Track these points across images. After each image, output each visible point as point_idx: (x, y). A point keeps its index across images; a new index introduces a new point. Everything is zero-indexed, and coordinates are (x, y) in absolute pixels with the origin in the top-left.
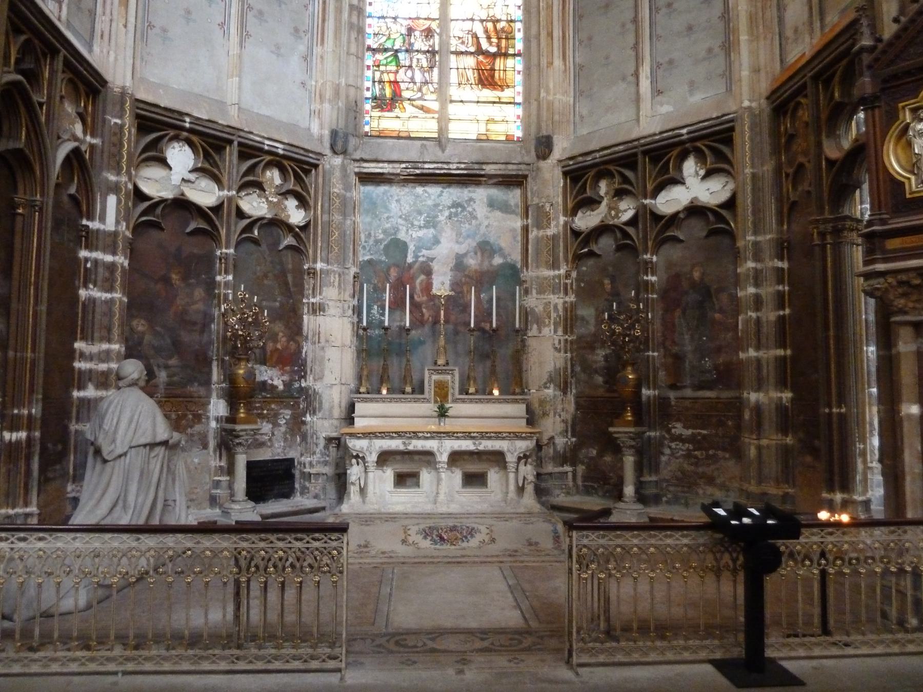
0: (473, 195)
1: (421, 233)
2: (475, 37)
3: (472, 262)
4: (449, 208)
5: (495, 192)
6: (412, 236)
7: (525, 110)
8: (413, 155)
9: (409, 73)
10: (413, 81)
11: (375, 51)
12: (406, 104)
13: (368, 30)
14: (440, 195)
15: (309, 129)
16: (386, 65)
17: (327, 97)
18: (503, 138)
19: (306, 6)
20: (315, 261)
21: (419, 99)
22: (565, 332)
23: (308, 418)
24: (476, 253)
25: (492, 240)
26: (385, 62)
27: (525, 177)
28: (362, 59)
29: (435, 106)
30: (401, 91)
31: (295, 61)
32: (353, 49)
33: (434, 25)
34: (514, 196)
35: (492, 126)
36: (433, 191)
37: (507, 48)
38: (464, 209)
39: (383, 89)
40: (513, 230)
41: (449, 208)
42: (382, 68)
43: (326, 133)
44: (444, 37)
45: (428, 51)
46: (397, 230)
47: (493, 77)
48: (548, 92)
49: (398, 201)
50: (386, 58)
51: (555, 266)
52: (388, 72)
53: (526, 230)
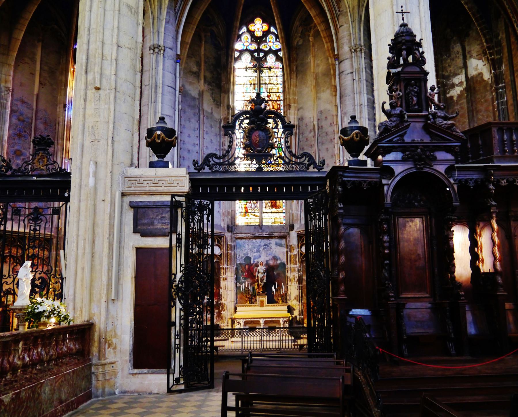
3: (271, 263)
5: (277, 240)
6: (252, 255)
7: (286, 215)
8: (252, 231)
9: (250, 205)
12: (249, 214)
20: (223, 265)
22: (299, 284)
23: (222, 312)
25: (277, 256)
29: (258, 214)
34: (283, 242)
35: (276, 220)
36: (259, 240)
38: (268, 246)
40: (284, 252)
43: (226, 226)
47: (276, 204)
48: (292, 210)
51: (295, 264)
53: (287, 252)
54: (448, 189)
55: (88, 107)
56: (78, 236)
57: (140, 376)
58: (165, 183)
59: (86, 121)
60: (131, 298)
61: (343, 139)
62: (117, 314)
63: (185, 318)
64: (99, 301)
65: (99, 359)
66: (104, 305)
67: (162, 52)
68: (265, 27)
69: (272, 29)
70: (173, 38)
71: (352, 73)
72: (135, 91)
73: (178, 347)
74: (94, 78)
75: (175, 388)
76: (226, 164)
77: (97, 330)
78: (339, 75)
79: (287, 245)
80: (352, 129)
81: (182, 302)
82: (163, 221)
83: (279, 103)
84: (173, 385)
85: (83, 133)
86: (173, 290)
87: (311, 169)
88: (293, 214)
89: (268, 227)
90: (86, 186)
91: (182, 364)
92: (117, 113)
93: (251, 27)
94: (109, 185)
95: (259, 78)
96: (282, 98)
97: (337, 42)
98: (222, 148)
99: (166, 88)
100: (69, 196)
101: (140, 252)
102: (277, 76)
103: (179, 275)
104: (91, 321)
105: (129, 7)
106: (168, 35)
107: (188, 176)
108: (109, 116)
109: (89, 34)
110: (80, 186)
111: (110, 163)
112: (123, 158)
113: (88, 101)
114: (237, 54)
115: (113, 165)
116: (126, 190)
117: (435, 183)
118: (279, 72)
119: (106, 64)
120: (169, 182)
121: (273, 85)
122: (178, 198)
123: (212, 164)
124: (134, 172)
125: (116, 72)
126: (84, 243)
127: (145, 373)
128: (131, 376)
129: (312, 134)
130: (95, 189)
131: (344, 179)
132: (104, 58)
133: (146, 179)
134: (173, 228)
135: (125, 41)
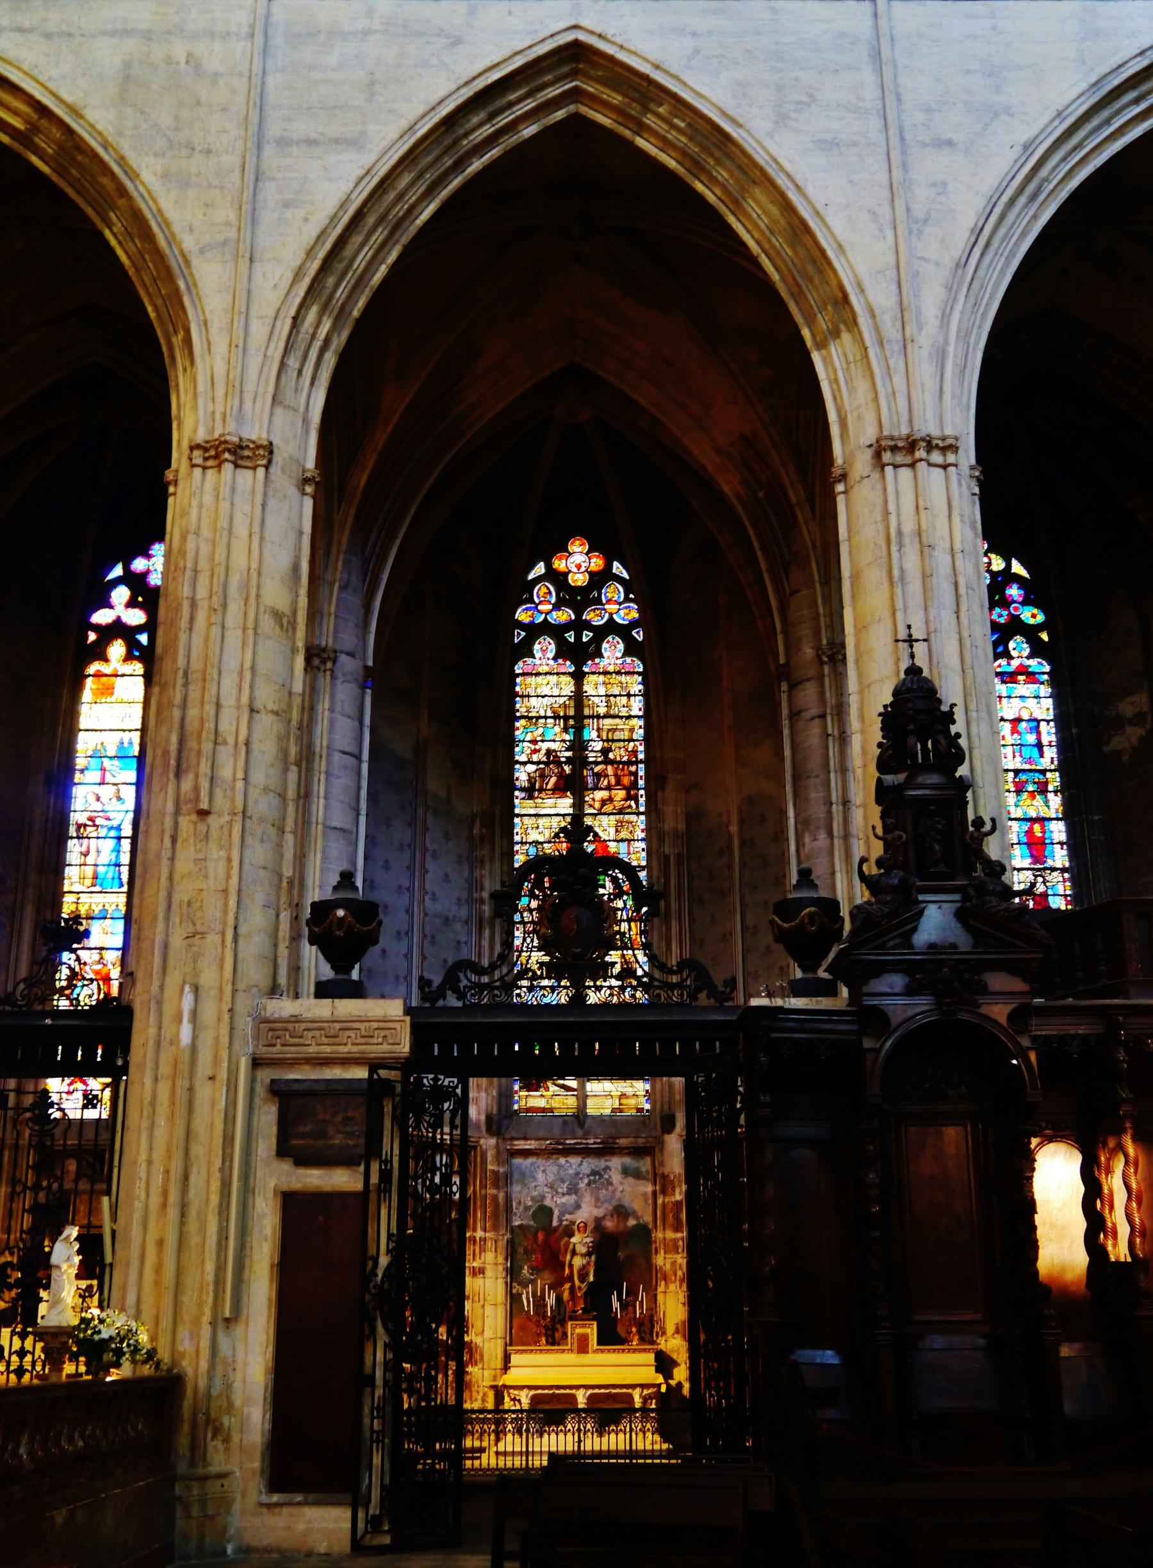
0: (609, 1164)
1: (564, 1200)
3: (609, 1224)
4: (588, 1176)
5: (627, 1160)
14: (580, 1165)
20: (475, 1230)
23: (469, 1369)
24: (612, 1216)
25: (626, 1204)
27: (654, 1148)
34: (645, 1164)
35: (624, 1101)
36: (574, 1160)
38: (601, 1176)
40: (645, 1194)
41: (588, 1176)
43: (483, 1117)
46: (543, 1197)
49: (544, 1171)
51: (677, 1229)
53: (654, 1193)
54: (1014, 1062)
55: (180, 855)
56: (150, 1162)
57: (285, 1510)
58: (353, 1036)
59: (176, 888)
60: (269, 1317)
61: (779, 926)
62: (234, 1356)
63: (392, 1367)
64: (196, 1322)
65: (192, 1464)
66: (206, 1331)
67: (329, 665)
68: (597, 563)
69: (617, 568)
70: (357, 626)
71: (823, 716)
72: (285, 810)
73: (378, 1437)
74: (196, 789)
75: (369, 1541)
76: (497, 988)
77: (189, 1392)
78: (790, 719)
79: (655, 1175)
80: (801, 903)
81: (390, 1325)
82: (348, 1129)
83: (633, 768)
84: (366, 1532)
85: (167, 918)
86: (367, 1298)
87: (703, 999)
89: (600, 1119)
90: (171, 1043)
91: (387, 1480)
92: (246, 867)
93: (559, 564)
94: (225, 1040)
96: (641, 756)
97: (785, 632)
98: (475, 895)
99: (337, 757)
100: (126, 1064)
101: (293, 1205)
102: (629, 695)
103: (384, 1261)
104: (175, 1371)
105: (277, 615)
106: (346, 620)
107: (408, 1019)
108: (228, 877)
109: (186, 684)
110: (158, 1044)
111: (228, 989)
112: (255, 973)
113: (180, 840)
114: (519, 636)
115: (234, 991)
116: (263, 1051)
117: (986, 1046)
118: (635, 685)
119: (225, 753)
120: (364, 1033)
121: (617, 721)
122: (383, 1073)
123: (465, 987)
124: (284, 1007)
125: (246, 772)
126: (166, 1180)
127: (299, 1504)
128: (264, 1510)
130: (194, 1048)
131: (774, 1035)
132: (220, 740)
133: (310, 1025)
134: (373, 1149)
135: (267, 696)
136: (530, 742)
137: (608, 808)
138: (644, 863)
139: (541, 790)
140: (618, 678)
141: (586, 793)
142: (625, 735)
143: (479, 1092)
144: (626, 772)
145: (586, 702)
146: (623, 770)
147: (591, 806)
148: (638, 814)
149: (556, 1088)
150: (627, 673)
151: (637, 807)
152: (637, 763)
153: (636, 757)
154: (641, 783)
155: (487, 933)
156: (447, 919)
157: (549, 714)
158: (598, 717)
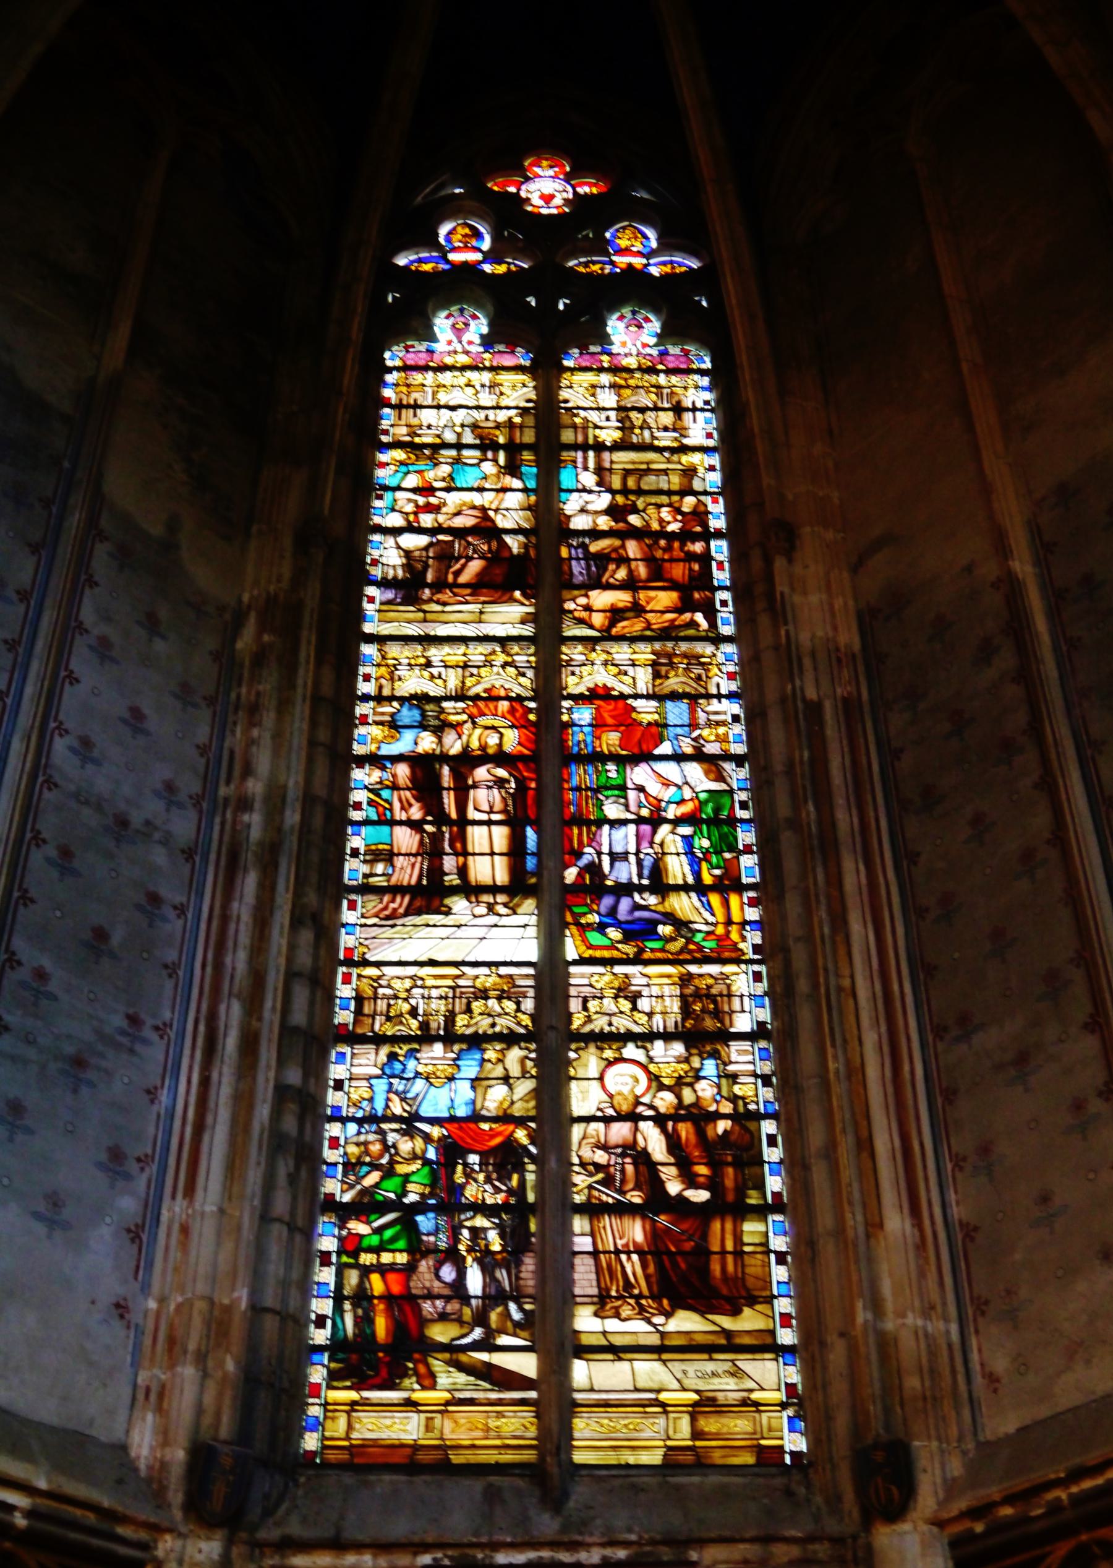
2: (643, 1159)
7: (808, 1372)
9: (448, 1273)
10: (458, 1289)
11: (344, 1212)
13: (330, 1155)
15: (124, 1448)
16: (377, 1250)
17: (192, 1346)
18: (749, 1459)
19: (152, 1094)
21: (476, 1346)
26: (375, 1240)
28: (309, 1234)
30: (423, 1322)
31: (104, 1239)
32: (281, 1204)
33: (521, 1135)
37: (741, 1191)
39: (365, 1321)
42: (367, 1259)
43: (179, 1455)
44: (553, 1164)
45: (505, 1207)
47: (706, 1270)
48: (876, 1305)
50: (379, 1231)
52: (383, 1270)
83: (698, 547)
88: (886, 1345)
95: (547, 411)
96: (718, 523)
98: (223, 791)
129: (1006, 660)
136: (414, 490)
137: (634, 626)
138: (740, 749)
139: (439, 586)
140: (653, 379)
141: (566, 594)
142: (676, 481)
143: (172, 1364)
144: (677, 553)
145: (565, 419)
146: (668, 549)
147: (581, 621)
148: (718, 640)
149: (462, 1378)
150: (669, 372)
151: (713, 624)
152: (707, 535)
153: (705, 525)
154: (721, 577)
155: (250, 883)
156: (123, 822)
157: (468, 438)
158: (599, 447)
